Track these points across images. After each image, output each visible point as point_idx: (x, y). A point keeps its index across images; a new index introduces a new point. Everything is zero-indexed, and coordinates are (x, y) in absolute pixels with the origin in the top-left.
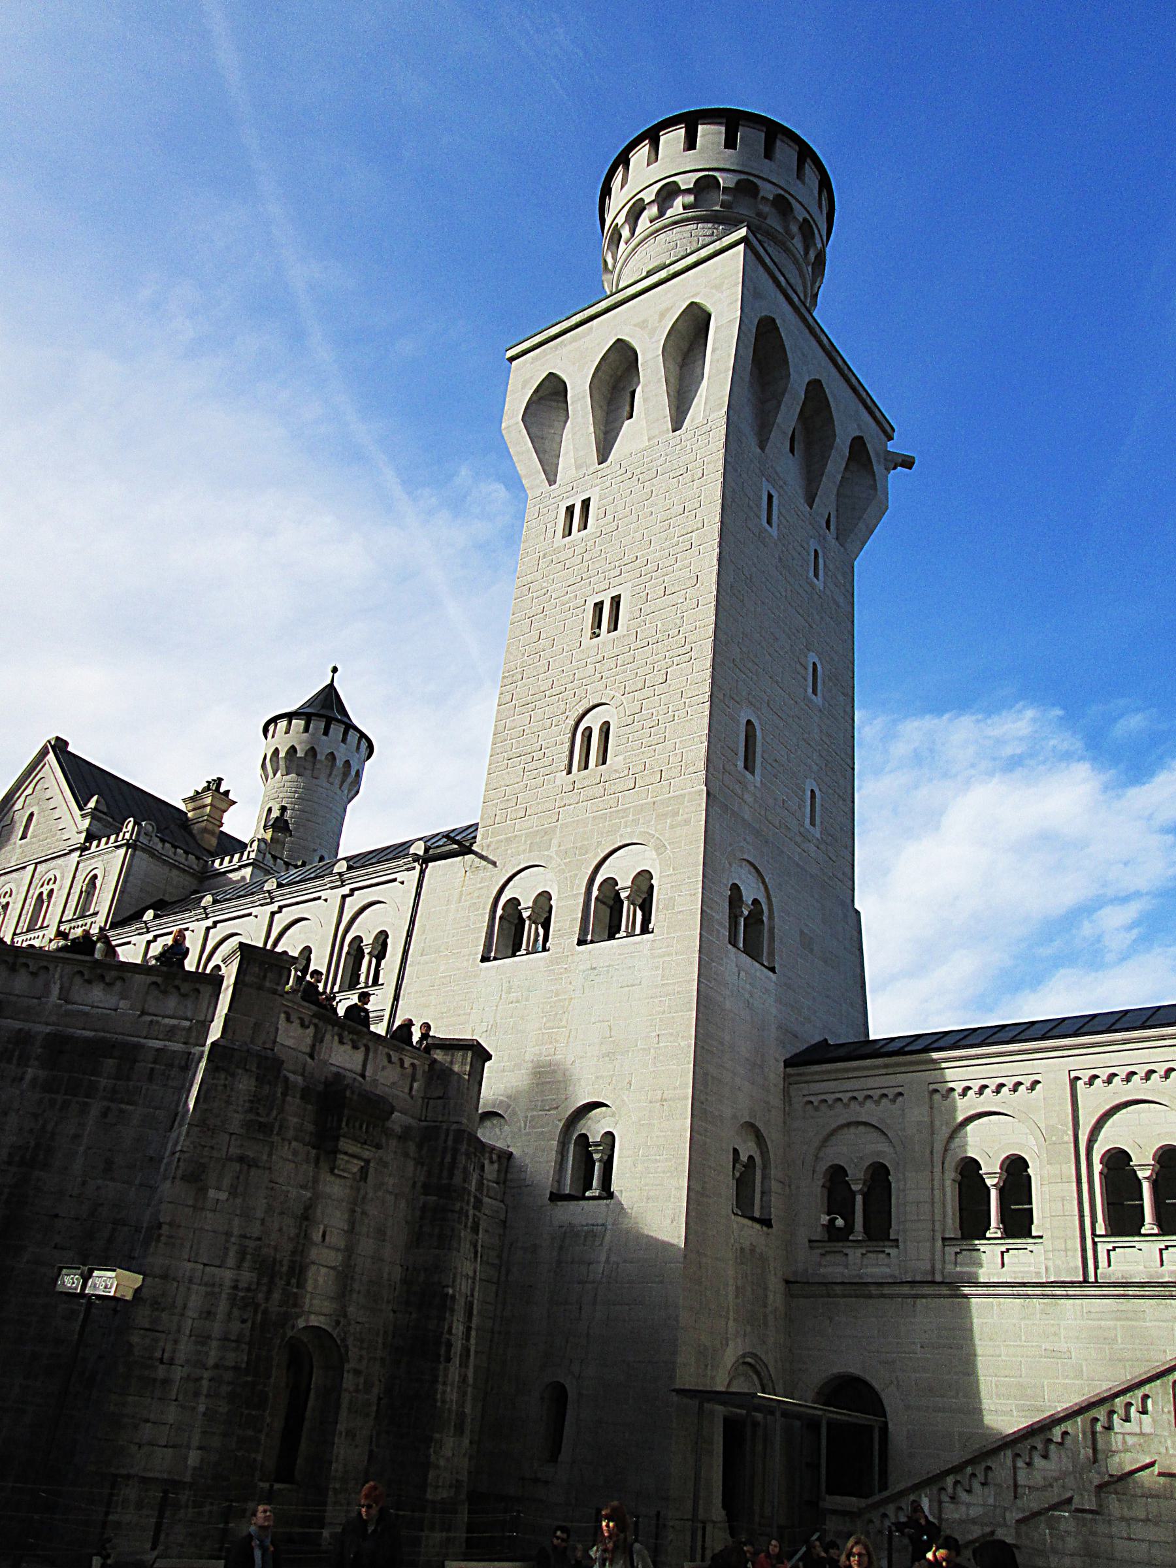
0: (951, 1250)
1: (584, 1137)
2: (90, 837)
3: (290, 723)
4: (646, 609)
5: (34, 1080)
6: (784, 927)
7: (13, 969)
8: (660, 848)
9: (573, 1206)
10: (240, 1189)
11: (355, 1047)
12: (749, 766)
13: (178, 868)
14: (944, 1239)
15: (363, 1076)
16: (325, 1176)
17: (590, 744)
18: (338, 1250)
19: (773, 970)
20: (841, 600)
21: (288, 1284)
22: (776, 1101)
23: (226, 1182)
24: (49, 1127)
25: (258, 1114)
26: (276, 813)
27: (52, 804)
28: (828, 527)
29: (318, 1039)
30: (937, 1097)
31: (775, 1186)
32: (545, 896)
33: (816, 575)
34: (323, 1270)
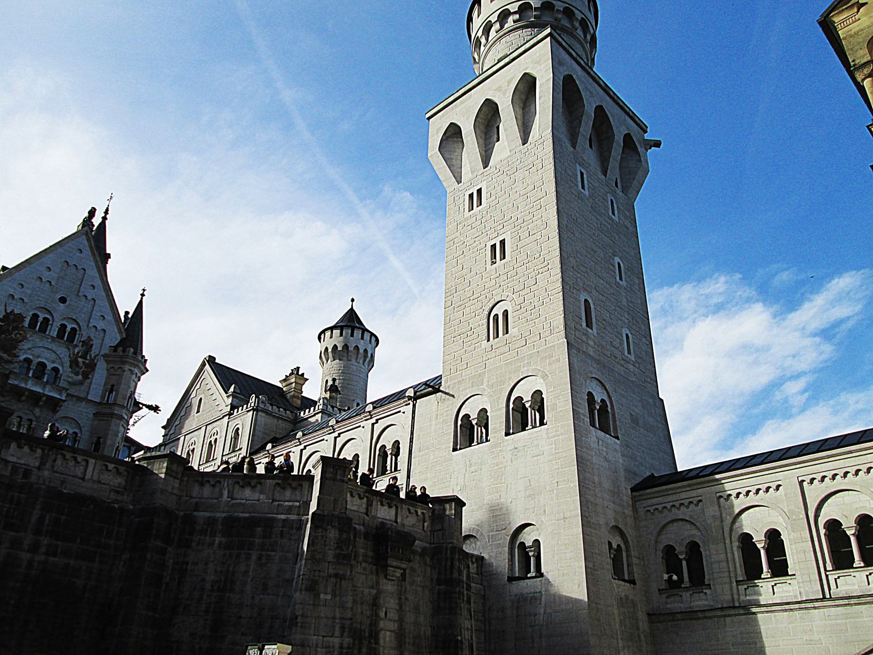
0: (742, 588)
1: (522, 544)
2: (233, 407)
3: (332, 333)
4: (520, 244)
5: (220, 543)
6: (620, 413)
7: (202, 484)
8: (545, 377)
9: (523, 583)
10: (338, 592)
11: (390, 507)
12: (589, 324)
13: (282, 419)
14: (737, 581)
15: (396, 522)
16: (383, 581)
17: (498, 324)
18: (395, 621)
19: (617, 438)
20: (629, 225)
21: (370, 642)
22: (628, 512)
23: (329, 589)
24: (231, 569)
25: (342, 550)
26: (330, 383)
27: (211, 392)
28: (617, 186)
29: (369, 504)
30: (722, 500)
31: (635, 560)
32: (484, 411)
33: (613, 213)
34: (388, 633)
